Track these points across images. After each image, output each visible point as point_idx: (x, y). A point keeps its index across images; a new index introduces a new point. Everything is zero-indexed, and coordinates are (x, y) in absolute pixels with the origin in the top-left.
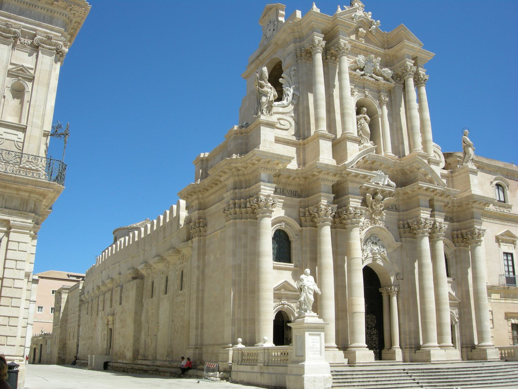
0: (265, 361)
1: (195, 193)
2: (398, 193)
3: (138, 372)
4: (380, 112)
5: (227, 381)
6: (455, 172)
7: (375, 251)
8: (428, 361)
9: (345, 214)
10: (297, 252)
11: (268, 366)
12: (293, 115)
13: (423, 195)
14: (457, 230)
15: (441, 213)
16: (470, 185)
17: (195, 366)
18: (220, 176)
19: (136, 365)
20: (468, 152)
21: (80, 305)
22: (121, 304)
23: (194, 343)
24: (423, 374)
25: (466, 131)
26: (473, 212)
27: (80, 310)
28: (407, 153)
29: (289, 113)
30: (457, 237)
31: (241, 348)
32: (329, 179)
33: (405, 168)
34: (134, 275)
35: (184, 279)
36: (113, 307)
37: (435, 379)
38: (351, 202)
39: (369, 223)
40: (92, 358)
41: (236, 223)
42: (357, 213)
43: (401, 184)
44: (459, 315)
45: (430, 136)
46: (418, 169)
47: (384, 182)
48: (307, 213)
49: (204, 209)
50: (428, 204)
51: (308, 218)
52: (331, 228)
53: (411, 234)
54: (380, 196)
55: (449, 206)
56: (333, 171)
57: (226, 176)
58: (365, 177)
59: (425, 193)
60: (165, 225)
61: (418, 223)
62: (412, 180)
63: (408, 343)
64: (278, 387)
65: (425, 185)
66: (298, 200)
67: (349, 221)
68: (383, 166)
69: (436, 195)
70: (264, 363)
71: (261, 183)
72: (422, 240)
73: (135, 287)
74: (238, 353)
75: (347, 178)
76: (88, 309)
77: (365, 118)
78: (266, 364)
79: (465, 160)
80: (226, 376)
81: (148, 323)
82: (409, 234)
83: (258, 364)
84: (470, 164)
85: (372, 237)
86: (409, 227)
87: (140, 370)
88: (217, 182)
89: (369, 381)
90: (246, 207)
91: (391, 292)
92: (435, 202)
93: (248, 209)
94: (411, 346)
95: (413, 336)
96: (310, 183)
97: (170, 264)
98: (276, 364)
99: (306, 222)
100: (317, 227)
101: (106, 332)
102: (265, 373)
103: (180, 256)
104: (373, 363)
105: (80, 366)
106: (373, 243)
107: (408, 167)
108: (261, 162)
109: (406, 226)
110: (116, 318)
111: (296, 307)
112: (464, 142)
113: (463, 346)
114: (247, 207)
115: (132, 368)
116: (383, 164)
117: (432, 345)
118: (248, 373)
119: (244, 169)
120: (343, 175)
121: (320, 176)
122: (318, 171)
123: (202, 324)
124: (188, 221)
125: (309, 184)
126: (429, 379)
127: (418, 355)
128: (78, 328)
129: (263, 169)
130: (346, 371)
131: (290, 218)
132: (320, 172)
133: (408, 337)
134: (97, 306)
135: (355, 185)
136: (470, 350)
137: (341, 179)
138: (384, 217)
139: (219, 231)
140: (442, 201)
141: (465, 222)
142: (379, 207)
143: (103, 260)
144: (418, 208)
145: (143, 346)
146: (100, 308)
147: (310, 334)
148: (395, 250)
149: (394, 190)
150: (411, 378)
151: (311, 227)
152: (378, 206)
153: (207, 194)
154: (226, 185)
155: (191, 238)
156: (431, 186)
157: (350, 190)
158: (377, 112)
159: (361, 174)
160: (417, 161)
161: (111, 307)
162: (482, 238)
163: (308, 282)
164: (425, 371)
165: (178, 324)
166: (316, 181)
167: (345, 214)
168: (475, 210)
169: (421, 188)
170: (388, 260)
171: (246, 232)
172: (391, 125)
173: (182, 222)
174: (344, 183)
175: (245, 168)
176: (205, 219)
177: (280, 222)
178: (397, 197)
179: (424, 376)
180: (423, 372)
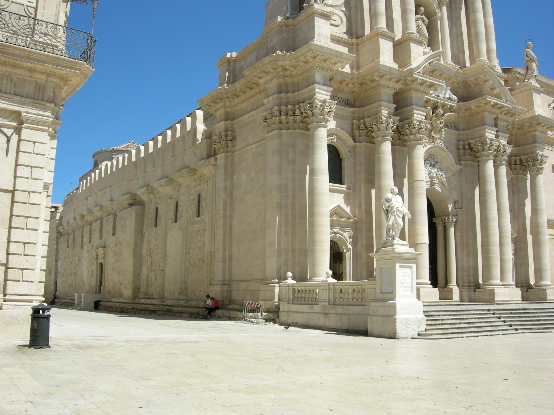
0: (329, 299)
1: (221, 99)
2: (460, 109)
3: (142, 312)
4: (439, 14)
5: (274, 323)
6: (515, 90)
7: (433, 174)
8: (491, 300)
9: (407, 129)
10: (350, 171)
11: (334, 305)
12: (344, 9)
13: (489, 112)
14: (515, 156)
15: (505, 135)
16: (533, 104)
17: (223, 305)
18: (260, 78)
19: (138, 305)
20: (532, 68)
21: (57, 238)
22: (114, 234)
23: (221, 279)
24: (511, 315)
25: (529, 43)
26: (535, 135)
27: (57, 243)
28: (468, 64)
29: (339, 6)
30: (515, 163)
31: (292, 284)
32: (390, 86)
33: (469, 80)
34: (131, 202)
35: (203, 204)
37: (527, 321)
38: (415, 115)
39: (428, 142)
40: (80, 297)
41: (281, 134)
42: (421, 128)
43: (462, 99)
44: (514, 250)
45: (493, 45)
46: (485, 81)
47: (445, 95)
48: (362, 126)
49: (233, 119)
50: (493, 123)
51: (363, 132)
52: (392, 145)
53: (471, 157)
54: (440, 111)
55: (509, 127)
56: (396, 76)
57: (268, 77)
58: (431, 86)
59: (491, 109)
60: (174, 141)
61: (482, 143)
62: (476, 94)
63: (466, 281)
64: (351, 330)
65: (493, 100)
66: (351, 110)
67: (412, 137)
68: (444, 76)
69: (501, 113)
70: (329, 301)
71: (316, 85)
72: (486, 163)
73: (134, 214)
74: (289, 290)
75: (411, 86)
76: (68, 241)
77: (422, 19)
78: (332, 303)
79: (528, 77)
80: (272, 318)
81: (151, 256)
82: (470, 156)
83: (320, 303)
84: (533, 81)
85: (430, 158)
86: (471, 148)
87: (144, 310)
88: (254, 85)
89: (460, 323)
90: (294, 115)
91: (449, 223)
92: (499, 121)
93: (297, 117)
94: (469, 284)
95: (471, 272)
96: (366, 91)
97: (180, 187)
98: (347, 303)
99: (360, 136)
100: (374, 144)
101: (94, 267)
102: (331, 313)
103: (196, 177)
104: (438, 302)
105: (60, 305)
106: (431, 165)
107: (472, 79)
108: (317, 60)
109: (467, 147)
110: (108, 252)
111: (349, 237)
112: (527, 56)
113: (518, 285)
114: (295, 114)
115: (134, 308)
116: (444, 73)
117: (495, 283)
118: (304, 314)
119: (292, 69)
120: (408, 82)
121: (381, 81)
122: (380, 75)
123: (231, 257)
124: (208, 136)
125: (364, 92)
126: (520, 321)
127: (478, 294)
129: (318, 68)
130: (431, 311)
131: (343, 131)
132: (381, 77)
133: (465, 273)
134: (81, 238)
135: (419, 95)
136: (526, 290)
137: (404, 86)
138: (443, 136)
139: (254, 146)
140: (506, 121)
141: (526, 146)
142: (439, 123)
143: (88, 185)
144: (483, 127)
145: (145, 282)
146: (86, 240)
147: (401, 267)
148: (454, 175)
149: (455, 105)
150: (499, 320)
151: (366, 142)
152: (439, 122)
153: (236, 101)
154: (265, 89)
155: (212, 155)
156: (499, 101)
157: (414, 101)
158: (436, 14)
159: (428, 82)
160: (485, 72)
161: (101, 238)
162: (544, 166)
163: (396, 203)
164: (513, 312)
165: (194, 257)
166: (375, 87)
167: (407, 129)
168: (538, 134)
169: (488, 103)
170: (447, 185)
171: (294, 146)
172: (451, 30)
173: (199, 136)
174: (406, 91)
175: (295, 67)
176: (233, 132)
177: (331, 135)
178: (458, 113)
179: (513, 317)
180: (511, 313)
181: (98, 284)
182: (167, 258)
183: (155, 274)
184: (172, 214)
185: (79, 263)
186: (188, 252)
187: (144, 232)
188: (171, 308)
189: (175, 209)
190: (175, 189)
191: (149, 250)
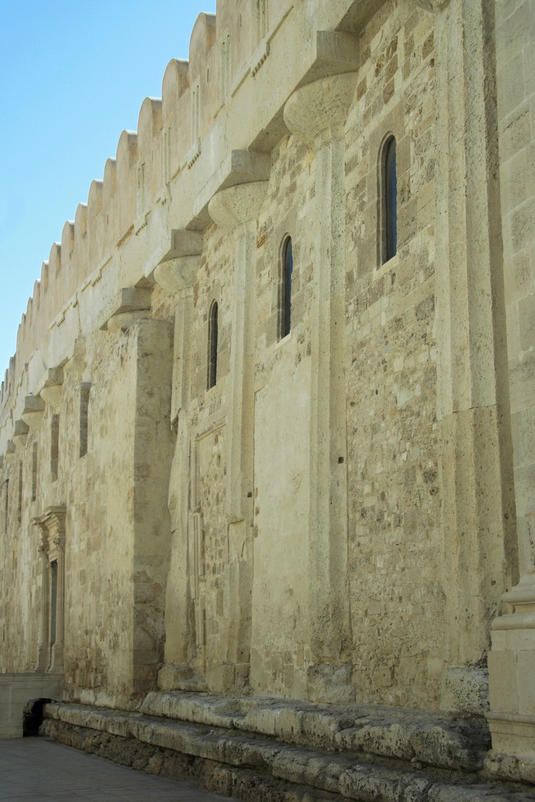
22: (83, 451)
81: (199, 510)
87: (162, 750)
146: (27, 493)
182: (259, 501)
183: (217, 584)
186: (344, 455)
187: (172, 418)
191: (193, 486)
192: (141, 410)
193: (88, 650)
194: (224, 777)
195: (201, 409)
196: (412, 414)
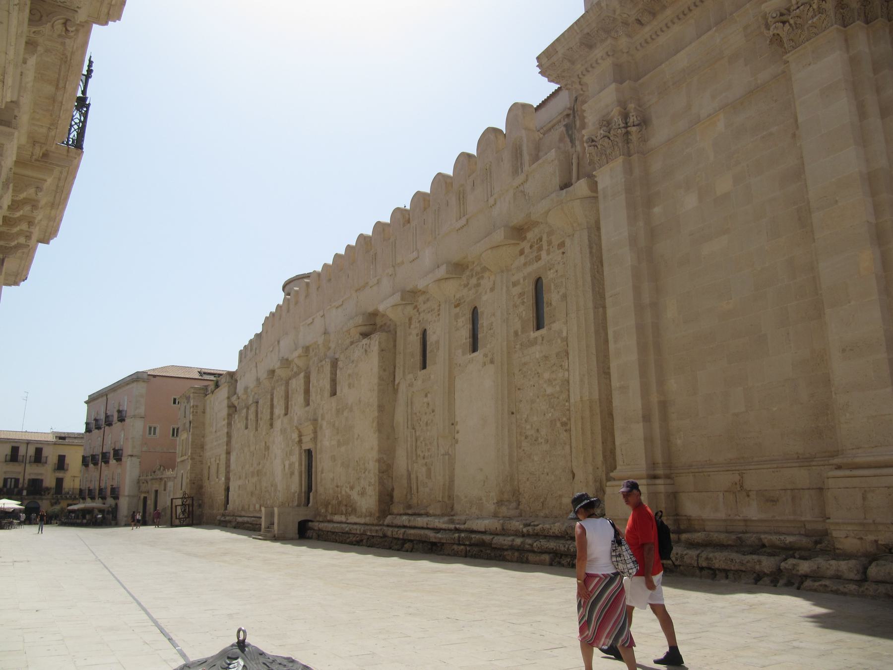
19: (396, 530)
21: (230, 416)
22: (334, 393)
27: (229, 425)
34: (364, 329)
36: (311, 403)
40: (271, 515)
73: (375, 348)
76: (247, 419)
81: (414, 428)
101: (295, 458)
103: (525, 245)
105: (235, 528)
110: (321, 427)
115: (385, 536)
123: (664, 405)
128: (226, 457)
134: (269, 411)
145: (405, 482)
146: (279, 410)
161: (307, 403)
181: (303, 490)
182: (457, 428)
183: (426, 464)
184: (464, 334)
185: (267, 453)
187: (397, 382)
188: (487, 538)
189: (470, 326)
190: (466, 286)
191: (409, 417)
192: (381, 378)
193: (339, 495)
194: (463, 549)
195: (415, 380)
196: (555, 397)
